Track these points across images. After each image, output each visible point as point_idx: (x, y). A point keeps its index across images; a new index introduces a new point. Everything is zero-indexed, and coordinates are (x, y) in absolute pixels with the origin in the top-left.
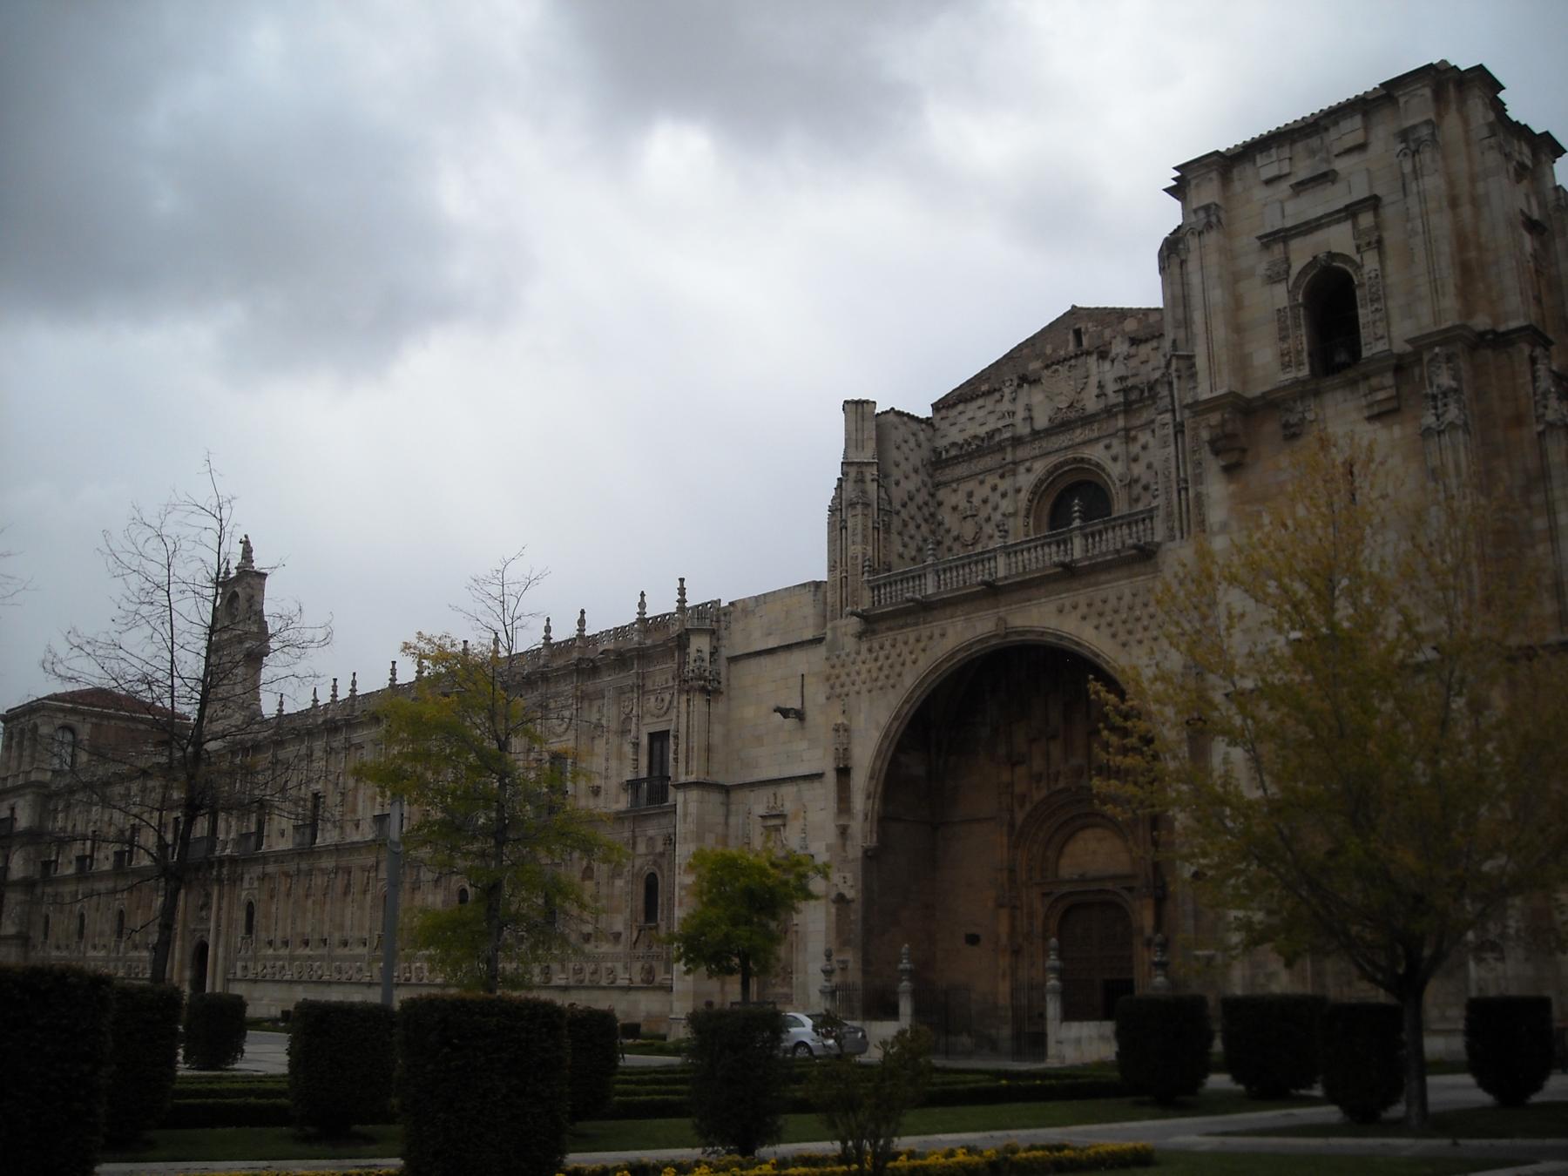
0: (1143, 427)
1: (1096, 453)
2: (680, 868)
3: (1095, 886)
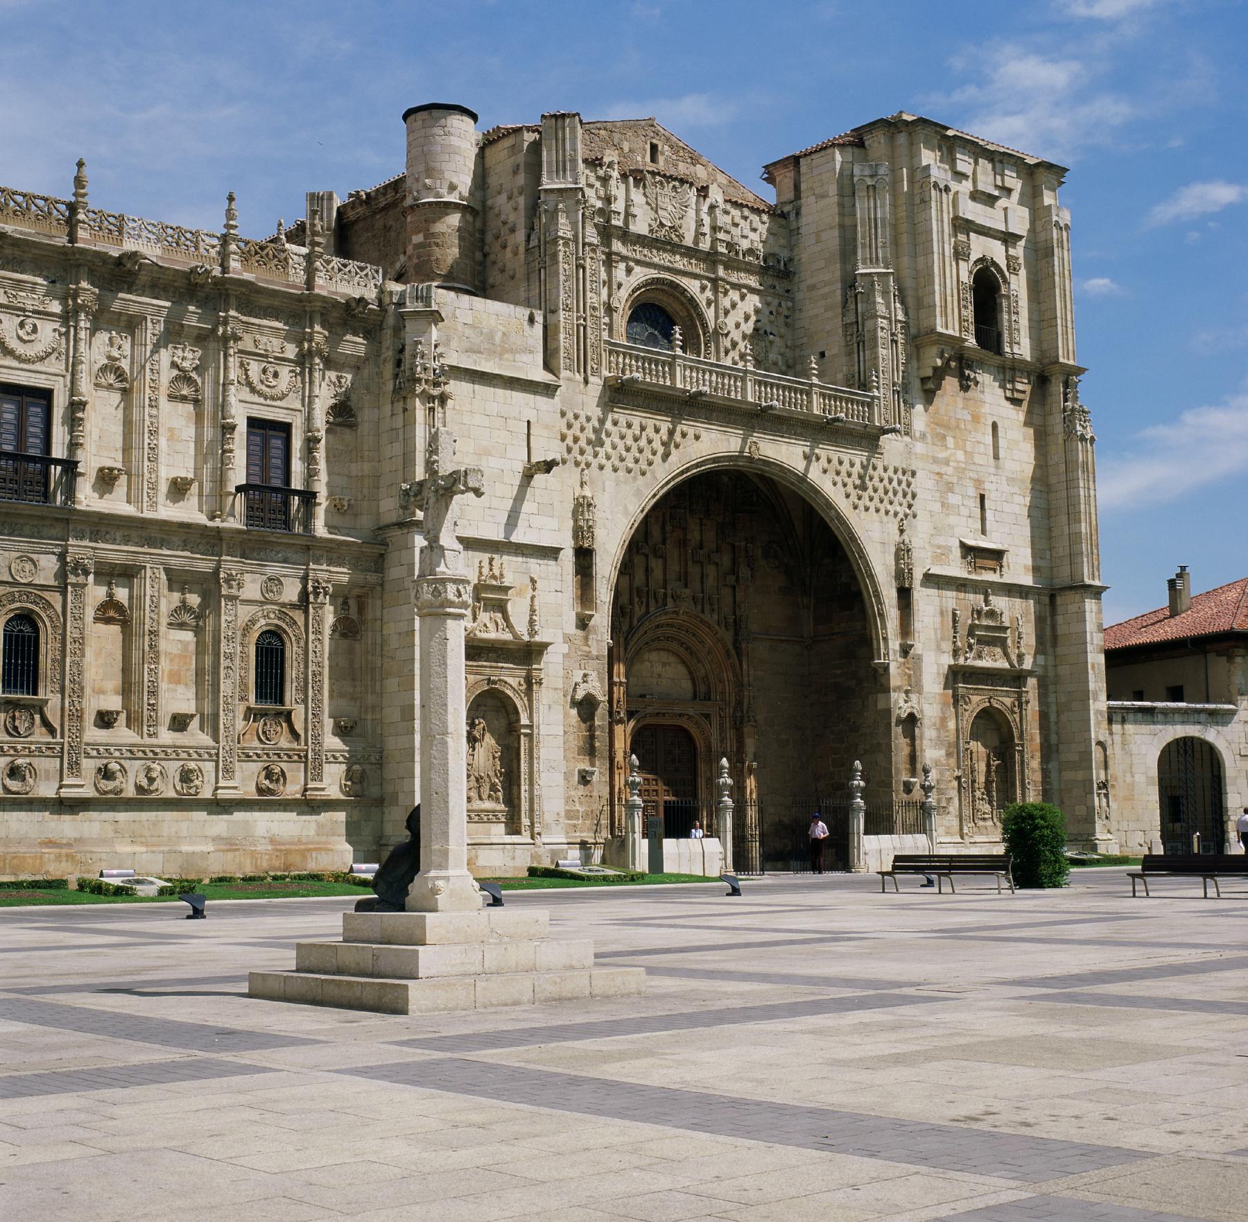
0: (736, 287)
1: (693, 286)
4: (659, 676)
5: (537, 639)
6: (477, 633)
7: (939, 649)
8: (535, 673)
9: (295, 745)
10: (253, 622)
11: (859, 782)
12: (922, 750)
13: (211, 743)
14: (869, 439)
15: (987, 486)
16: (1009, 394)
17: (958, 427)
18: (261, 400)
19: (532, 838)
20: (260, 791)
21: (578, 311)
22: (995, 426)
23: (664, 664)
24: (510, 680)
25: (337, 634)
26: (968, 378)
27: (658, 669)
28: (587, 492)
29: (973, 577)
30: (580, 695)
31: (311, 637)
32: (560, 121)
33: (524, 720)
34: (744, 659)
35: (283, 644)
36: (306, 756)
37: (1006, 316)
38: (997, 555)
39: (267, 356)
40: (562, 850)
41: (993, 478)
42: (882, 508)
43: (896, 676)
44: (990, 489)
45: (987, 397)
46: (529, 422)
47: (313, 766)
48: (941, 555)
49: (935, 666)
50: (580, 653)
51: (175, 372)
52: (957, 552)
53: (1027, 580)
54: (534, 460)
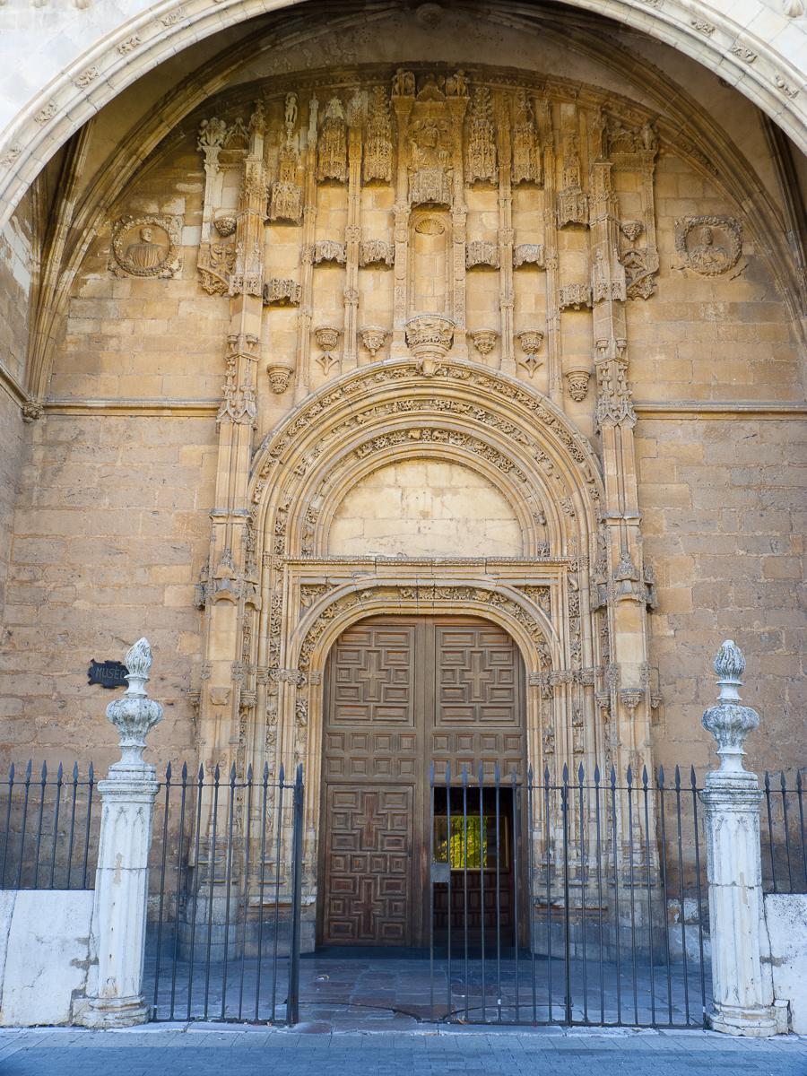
3: (446, 578)
4: (425, 515)
23: (439, 492)
27: (421, 500)
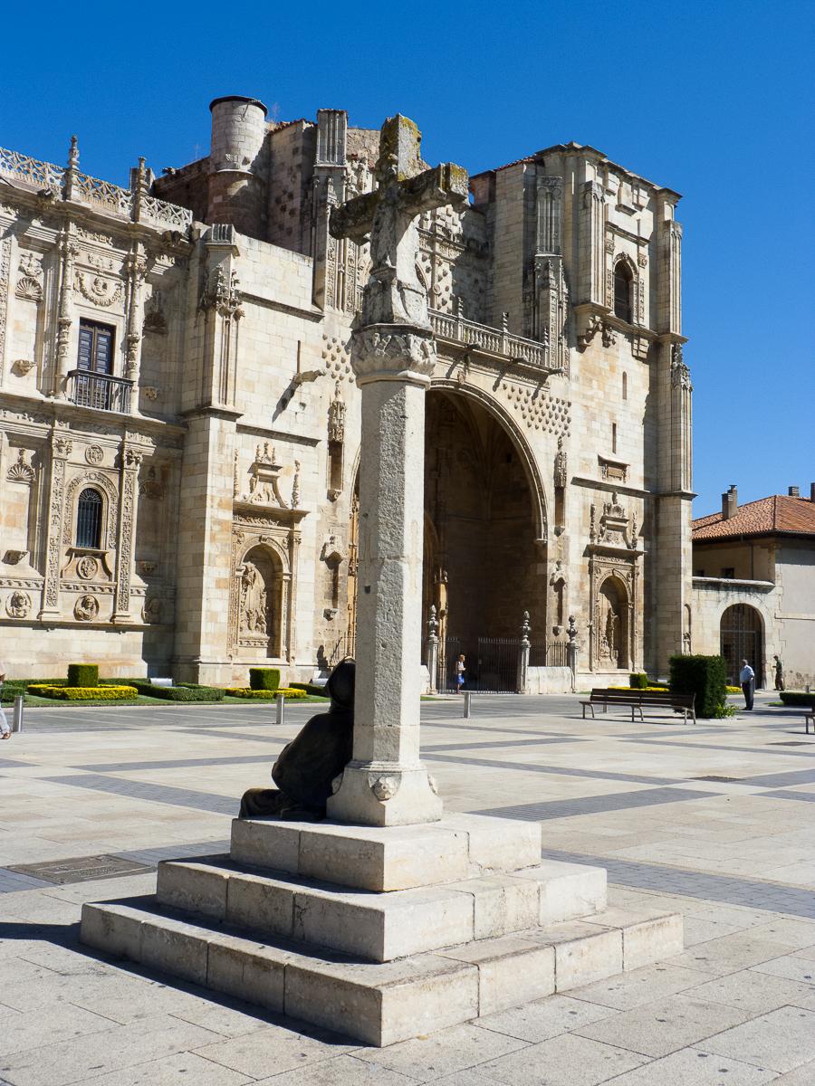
2: (212, 500)
5: (299, 508)
6: (253, 500)
7: (581, 533)
8: (295, 534)
9: (107, 581)
10: (77, 481)
11: (527, 627)
12: (566, 606)
13: (38, 576)
14: (540, 378)
15: (618, 418)
16: (635, 354)
17: (600, 374)
18: (92, 305)
19: (288, 660)
20: (77, 616)
21: (339, 261)
22: (625, 375)
24: (276, 539)
25: (144, 495)
26: (609, 339)
28: (340, 399)
29: (606, 482)
30: (328, 554)
31: (124, 495)
32: (332, 115)
33: (286, 570)
34: (442, 534)
35: (101, 500)
36: (116, 590)
37: (635, 298)
38: (623, 467)
39: (98, 271)
40: (310, 671)
41: (622, 413)
42: (547, 427)
43: (552, 553)
44: (619, 419)
45: (620, 354)
46: (299, 342)
47: (120, 598)
48: (585, 464)
49: (578, 545)
50: (329, 521)
51: (22, 275)
52: (596, 462)
53: (641, 487)
54: (302, 371)
